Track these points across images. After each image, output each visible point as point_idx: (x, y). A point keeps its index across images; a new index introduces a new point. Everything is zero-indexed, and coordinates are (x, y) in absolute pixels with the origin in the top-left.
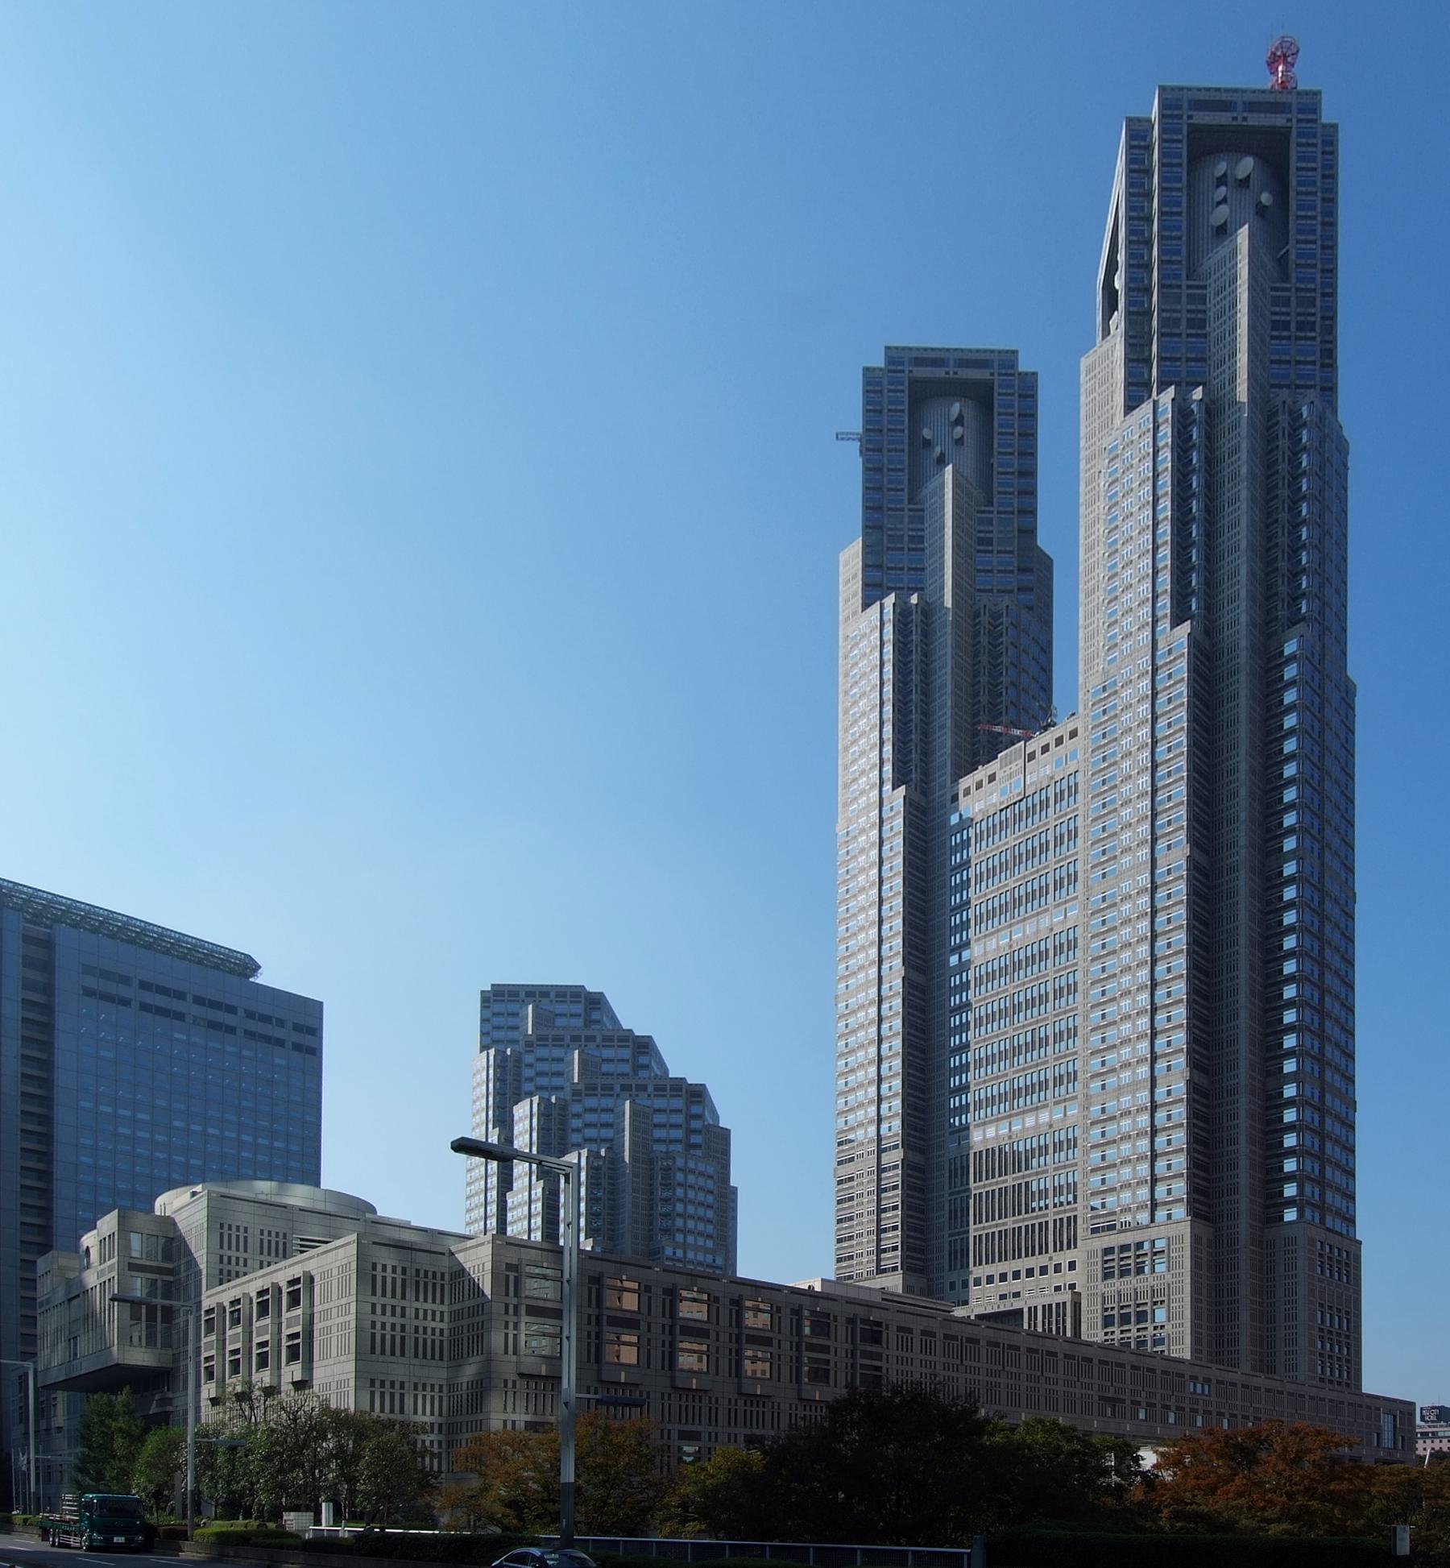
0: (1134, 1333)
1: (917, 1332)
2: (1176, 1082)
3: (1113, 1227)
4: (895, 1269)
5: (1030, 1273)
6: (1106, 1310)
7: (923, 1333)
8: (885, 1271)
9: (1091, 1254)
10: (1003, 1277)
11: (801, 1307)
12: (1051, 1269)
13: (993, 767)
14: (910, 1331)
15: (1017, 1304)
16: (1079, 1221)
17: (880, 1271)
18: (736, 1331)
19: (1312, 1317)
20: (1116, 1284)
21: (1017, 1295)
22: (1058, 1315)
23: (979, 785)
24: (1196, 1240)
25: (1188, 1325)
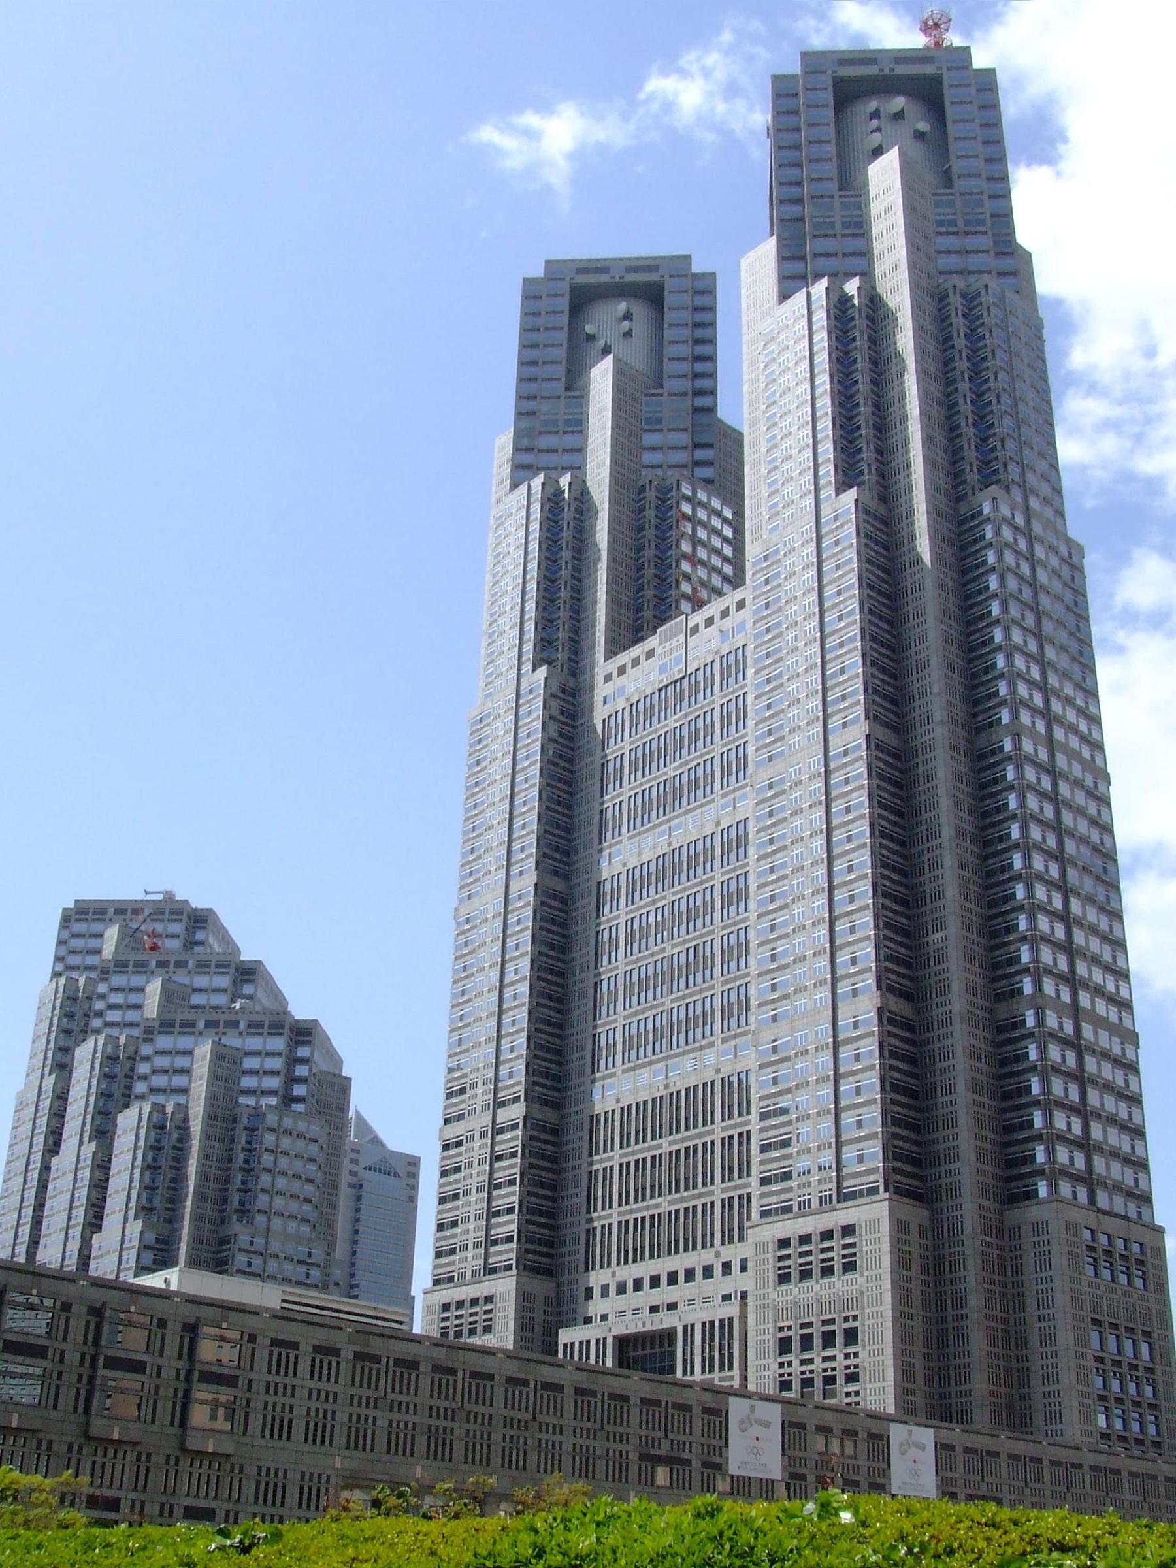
0: (818, 1365)
1: (305, 1348)
2: (864, 1006)
3: (789, 1209)
4: (508, 1268)
5: (690, 1275)
6: (781, 1329)
7: (317, 1349)
8: (493, 1271)
9: (761, 1247)
10: (655, 1282)
11: (104, 1304)
12: (718, 1270)
13: (652, 642)
14: (295, 1345)
15: (666, 1320)
16: (754, 1200)
17: (491, 1271)
18: (92, 1350)
19: (1081, 1341)
20: (795, 1291)
21: (672, 1306)
22: (722, 1336)
23: (636, 662)
24: (900, 1228)
25: (889, 1351)
